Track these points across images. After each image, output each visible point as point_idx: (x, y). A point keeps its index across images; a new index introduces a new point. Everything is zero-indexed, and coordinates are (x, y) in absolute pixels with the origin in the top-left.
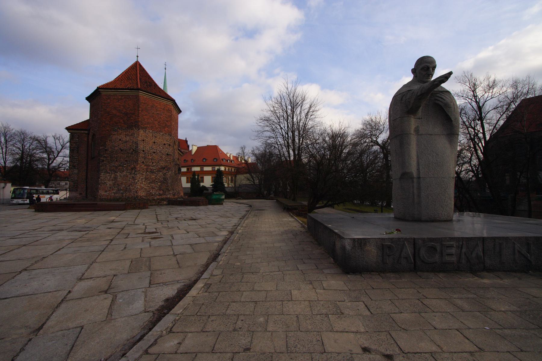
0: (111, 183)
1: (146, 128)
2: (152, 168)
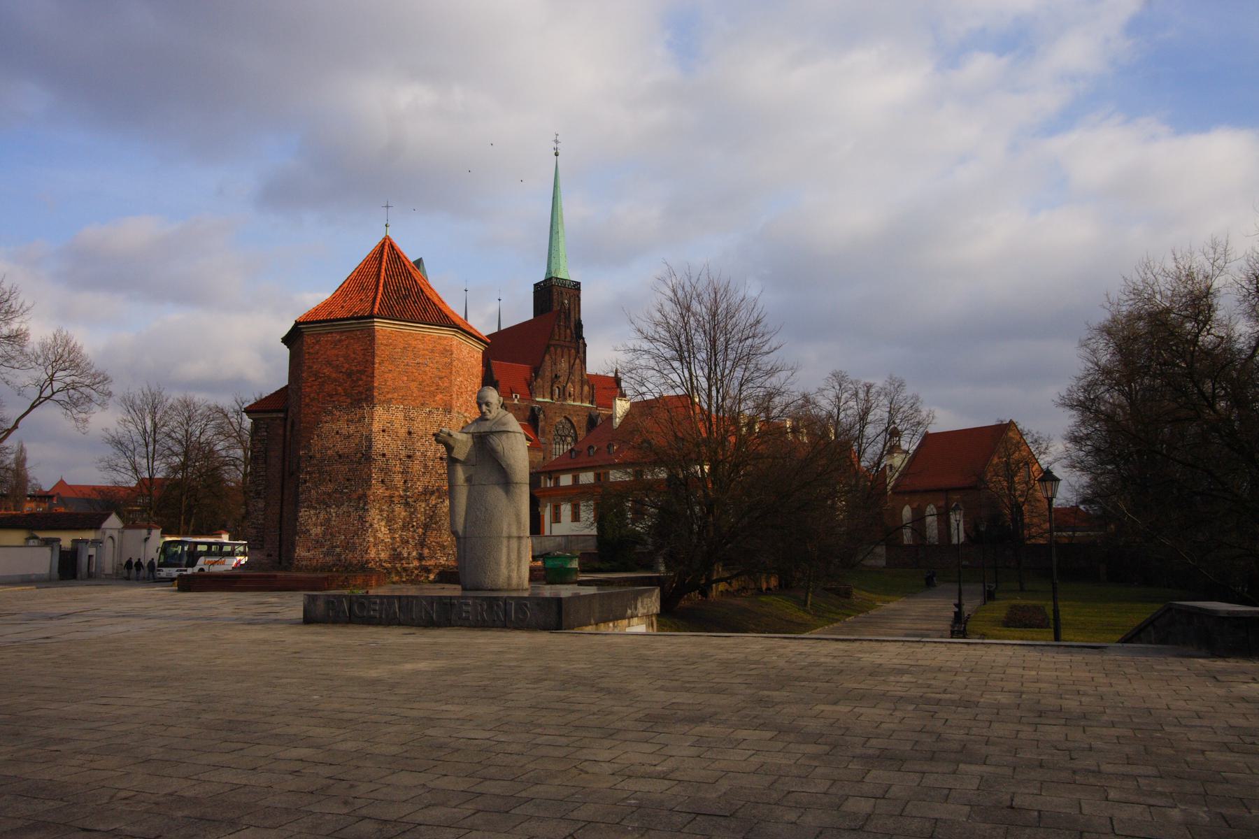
0: (319, 530)
1: (389, 401)
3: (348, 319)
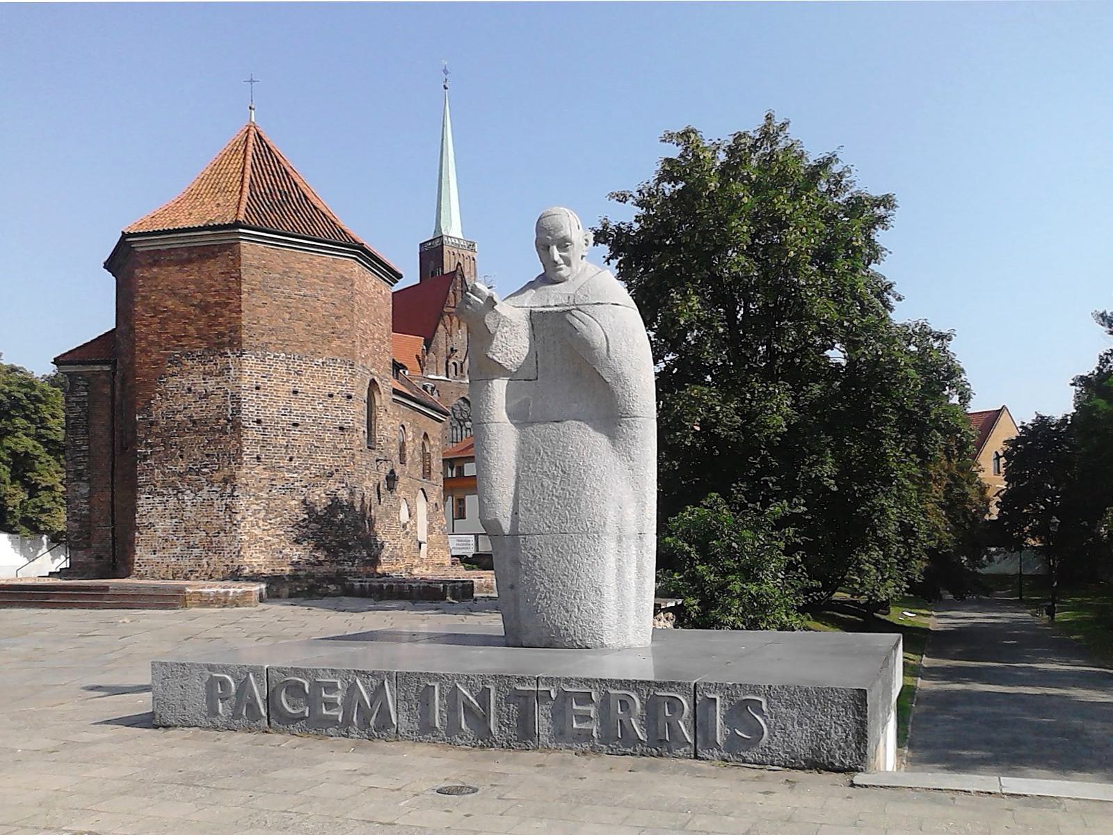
1: (265, 347)
3: (199, 229)
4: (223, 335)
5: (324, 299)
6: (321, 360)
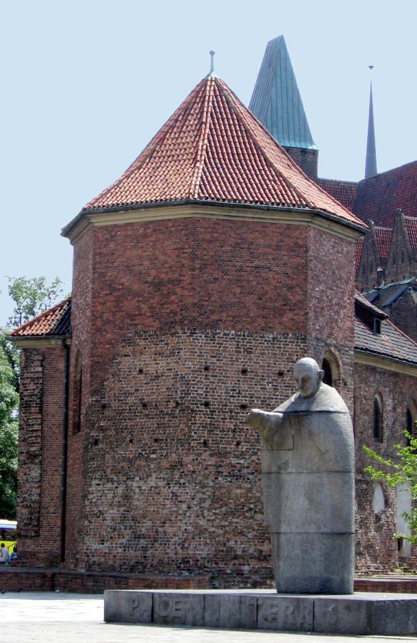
1: (214, 325)
2: (234, 461)
4: (175, 314)
5: (276, 269)
6: (271, 336)
